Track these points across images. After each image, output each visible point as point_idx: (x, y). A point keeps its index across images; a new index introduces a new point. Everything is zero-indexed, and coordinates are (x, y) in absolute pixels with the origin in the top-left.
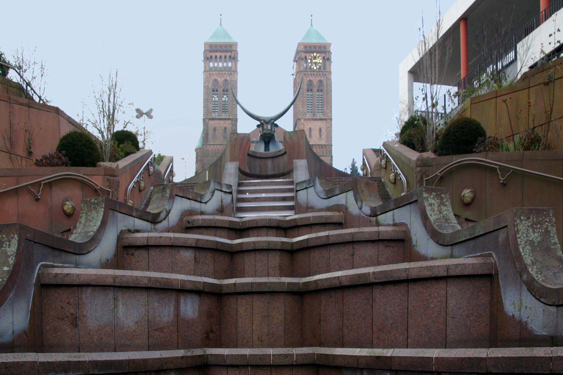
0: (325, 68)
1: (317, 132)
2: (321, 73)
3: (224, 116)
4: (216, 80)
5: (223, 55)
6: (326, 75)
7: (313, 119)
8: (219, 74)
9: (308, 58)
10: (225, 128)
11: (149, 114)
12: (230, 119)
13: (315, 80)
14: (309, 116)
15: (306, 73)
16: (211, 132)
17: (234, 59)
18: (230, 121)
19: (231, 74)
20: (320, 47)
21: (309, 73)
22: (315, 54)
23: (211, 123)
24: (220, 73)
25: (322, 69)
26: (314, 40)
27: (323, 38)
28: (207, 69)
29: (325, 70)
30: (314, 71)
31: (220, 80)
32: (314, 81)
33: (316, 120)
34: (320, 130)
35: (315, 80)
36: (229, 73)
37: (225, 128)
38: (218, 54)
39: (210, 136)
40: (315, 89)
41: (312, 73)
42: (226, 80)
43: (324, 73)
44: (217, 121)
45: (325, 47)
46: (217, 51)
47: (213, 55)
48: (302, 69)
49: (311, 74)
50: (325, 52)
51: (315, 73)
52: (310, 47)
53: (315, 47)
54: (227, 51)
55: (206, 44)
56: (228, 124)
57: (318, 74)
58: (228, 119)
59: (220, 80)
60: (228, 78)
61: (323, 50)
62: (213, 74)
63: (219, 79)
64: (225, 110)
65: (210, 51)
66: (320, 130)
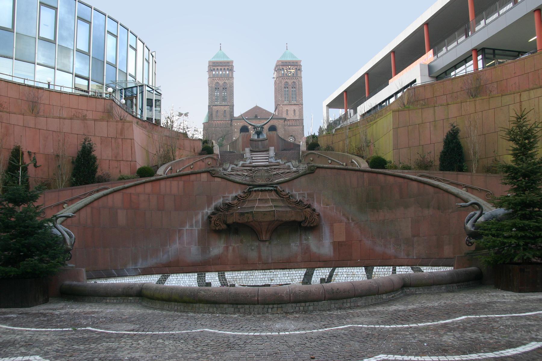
0: (297, 75)
1: (292, 112)
3: (224, 103)
5: (223, 68)
7: (289, 105)
11: (186, 115)
13: (290, 82)
14: (286, 102)
16: (214, 113)
17: (231, 70)
20: (293, 62)
23: (214, 107)
25: (295, 75)
26: (289, 59)
27: (296, 57)
28: (211, 76)
29: (297, 76)
30: (289, 76)
31: (221, 83)
33: (291, 105)
34: (294, 110)
35: (290, 82)
38: (219, 68)
39: (214, 115)
45: (297, 62)
47: (216, 68)
48: (280, 75)
50: (297, 66)
52: (286, 62)
53: (289, 62)
54: (225, 66)
55: (210, 62)
56: (227, 108)
59: (221, 83)
60: (227, 81)
61: (296, 65)
63: (220, 82)
64: (224, 99)
65: (213, 66)
66: (294, 110)
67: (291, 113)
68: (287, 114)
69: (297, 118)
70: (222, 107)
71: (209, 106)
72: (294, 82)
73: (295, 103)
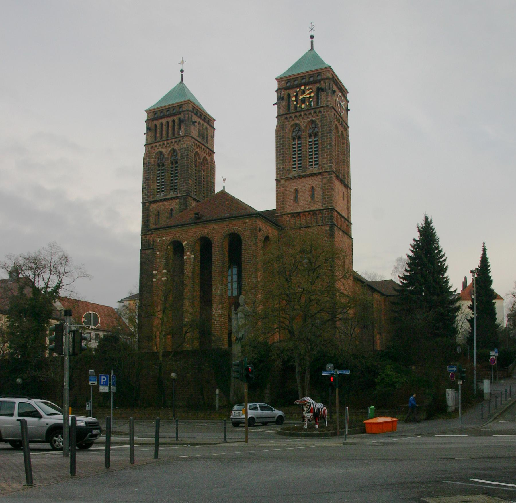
2: (312, 111)
4: (161, 153)
6: (320, 112)
8: (164, 144)
9: (292, 95)
10: (172, 210)
12: (178, 198)
15: (288, 116)
18: (178, 200)
19: (180, 141)
20: (311, 76)
21: (293, 115)
22: (303, 88)
23: (154, 206)
24: (166, 142)
30: (302, 110)
31: (165, 151)
32: (301, 124)
36: (177, 140)
37: (172, 210)
40: (305, 134)
41: (298, 114)
42: (174, 150)
43: (318, 110)
44: (161, 203)
46: (161, 118)
49: (296, 116)
51: (303, 113)
54: (174, 115)
57: (307, 113)
58: (174, 198)
60: (176, 147)
62: (156, 146)
63: (164, 151)
67: (305, 196)
68: (296, 199)
69: (318, 206)
70: (165, 203)
71: (144, 204)
72: (313, 122)
73: (316, 170)
